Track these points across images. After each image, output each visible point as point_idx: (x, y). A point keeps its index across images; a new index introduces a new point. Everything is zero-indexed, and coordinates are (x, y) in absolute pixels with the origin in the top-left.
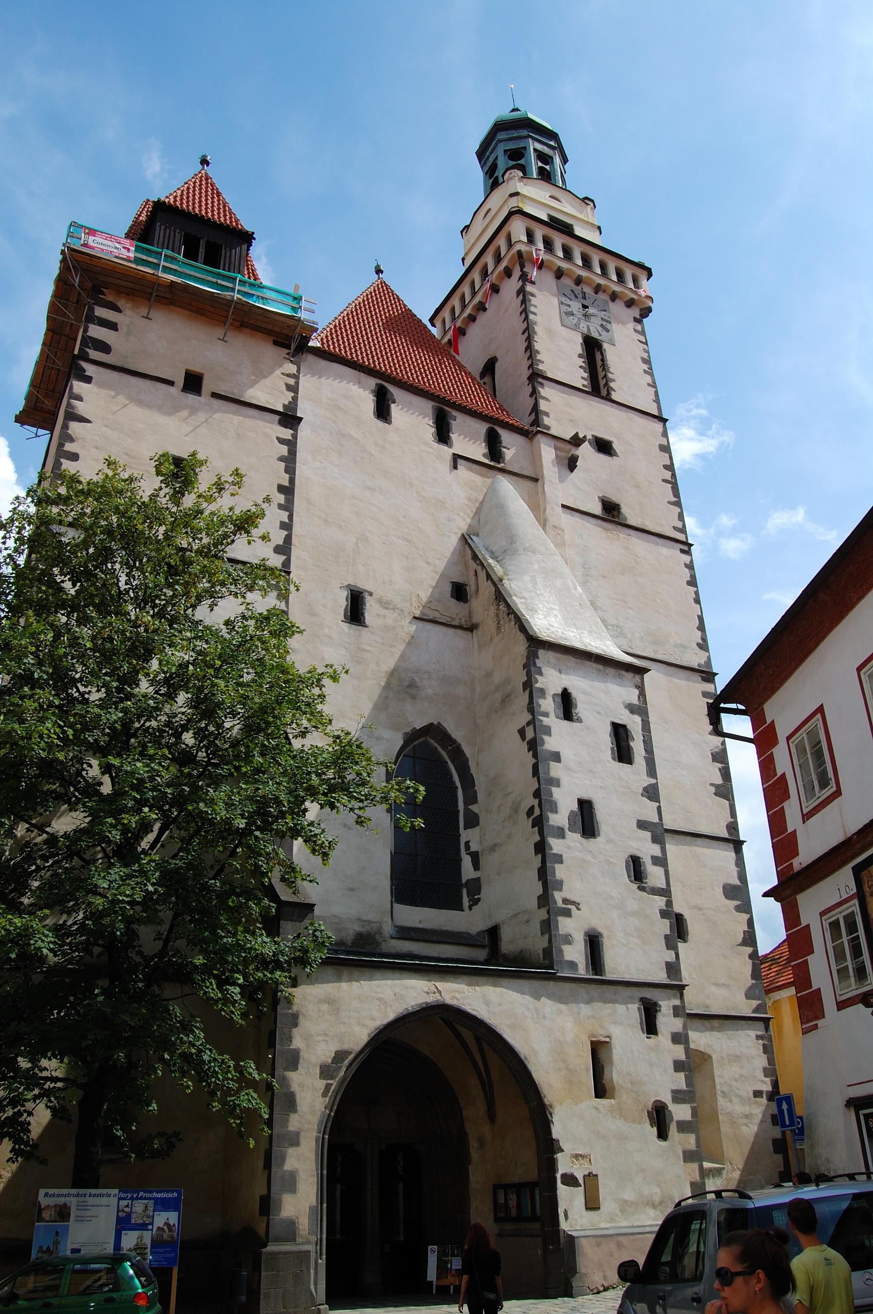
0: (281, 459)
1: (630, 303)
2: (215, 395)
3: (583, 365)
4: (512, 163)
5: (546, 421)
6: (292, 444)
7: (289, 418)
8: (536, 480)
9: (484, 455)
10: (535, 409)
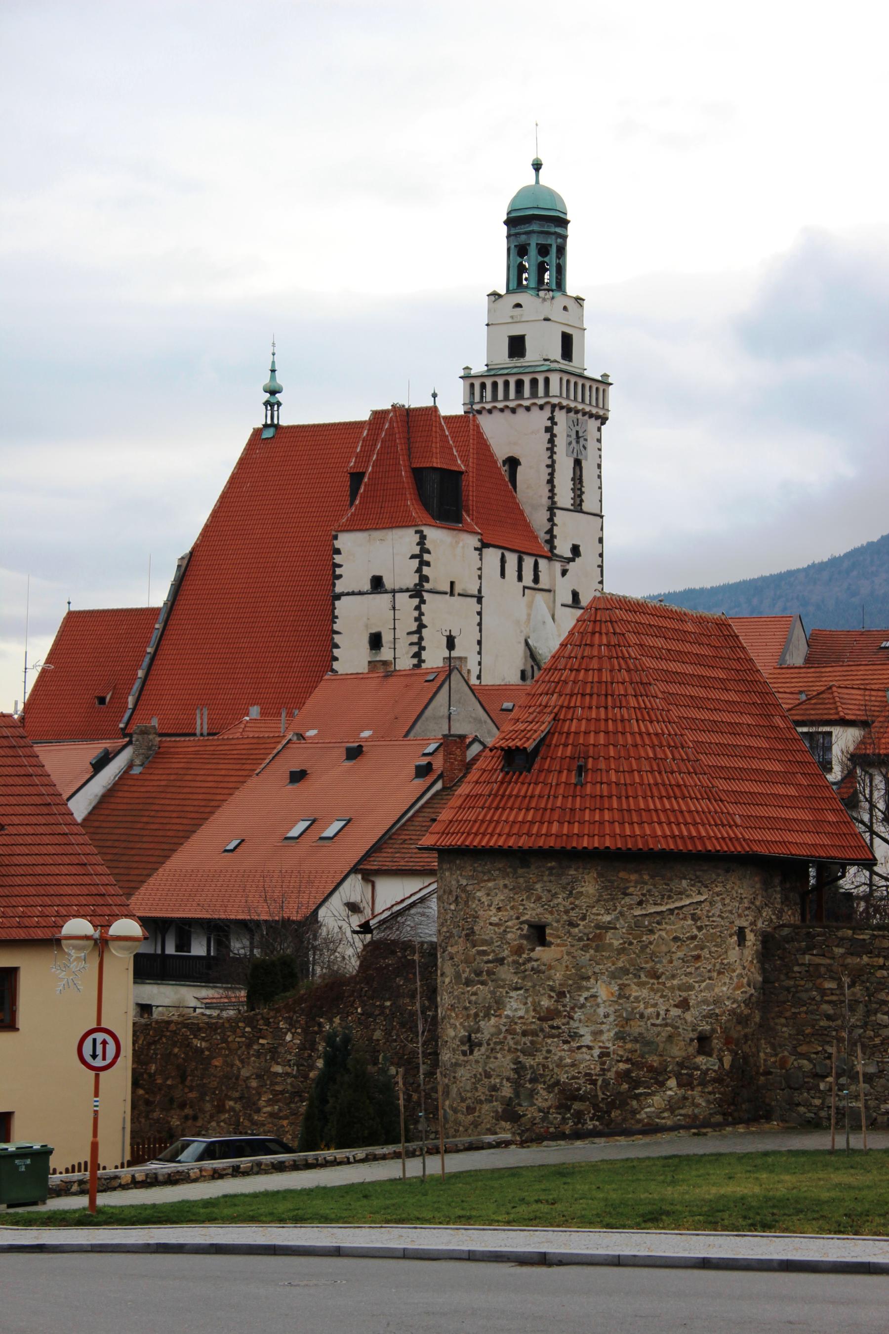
1: (597, 417)
2: (459, 595)
4: (540, 259)
8: (549, 591)
10: (550, 531)
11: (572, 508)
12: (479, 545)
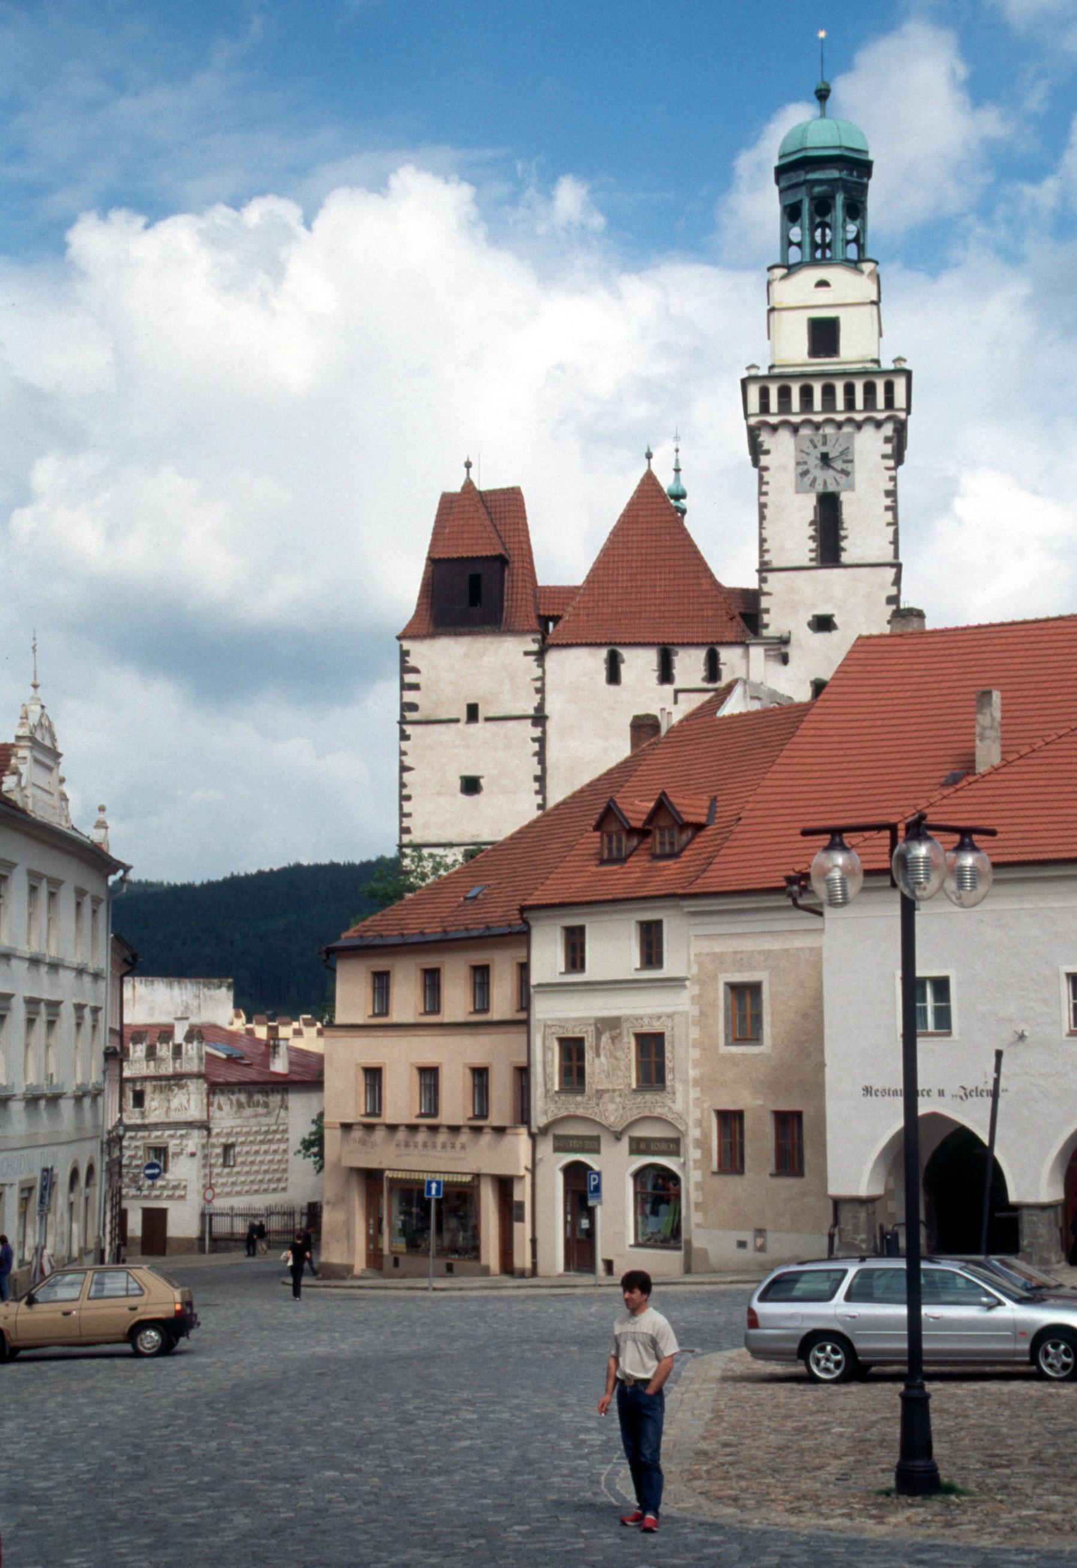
0: (536, 754)
1: (879, 424)
2: (488, 719)
3: (813, 533)
5: (766, 618)
6: (541, 741)
7: (539, 718)
9: (705, 679)
11: (813, 564)
12: (535, 647)
